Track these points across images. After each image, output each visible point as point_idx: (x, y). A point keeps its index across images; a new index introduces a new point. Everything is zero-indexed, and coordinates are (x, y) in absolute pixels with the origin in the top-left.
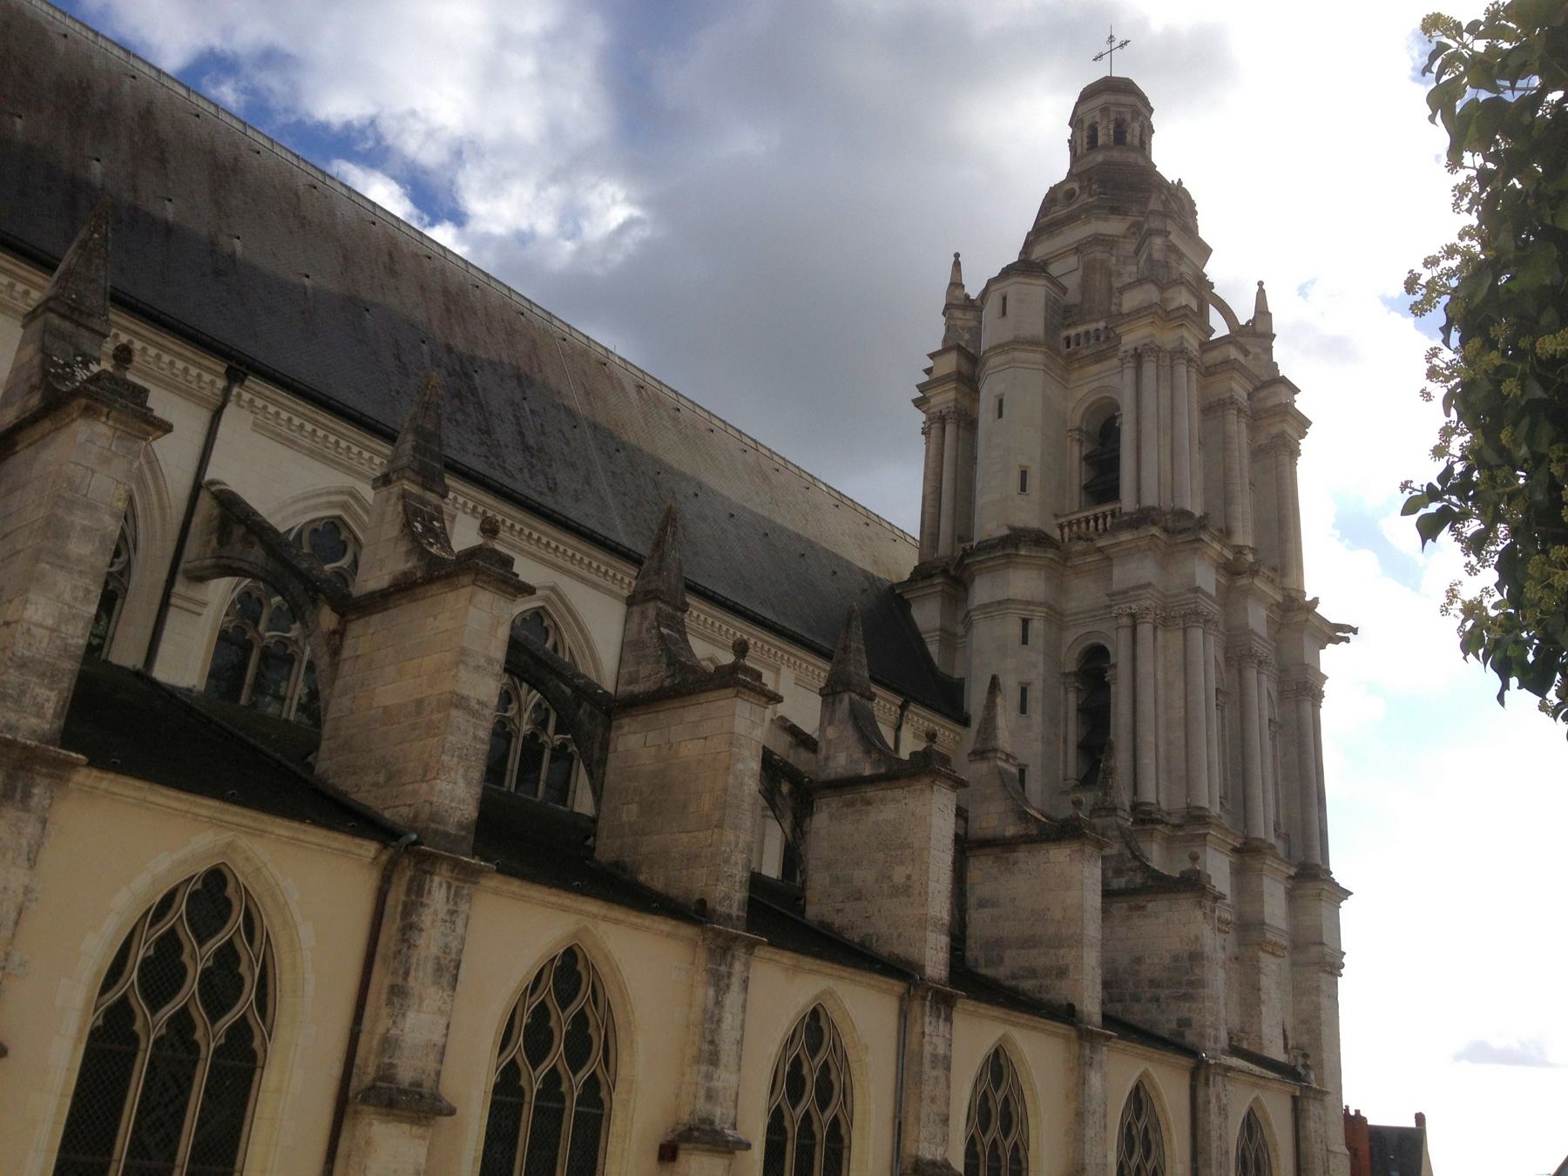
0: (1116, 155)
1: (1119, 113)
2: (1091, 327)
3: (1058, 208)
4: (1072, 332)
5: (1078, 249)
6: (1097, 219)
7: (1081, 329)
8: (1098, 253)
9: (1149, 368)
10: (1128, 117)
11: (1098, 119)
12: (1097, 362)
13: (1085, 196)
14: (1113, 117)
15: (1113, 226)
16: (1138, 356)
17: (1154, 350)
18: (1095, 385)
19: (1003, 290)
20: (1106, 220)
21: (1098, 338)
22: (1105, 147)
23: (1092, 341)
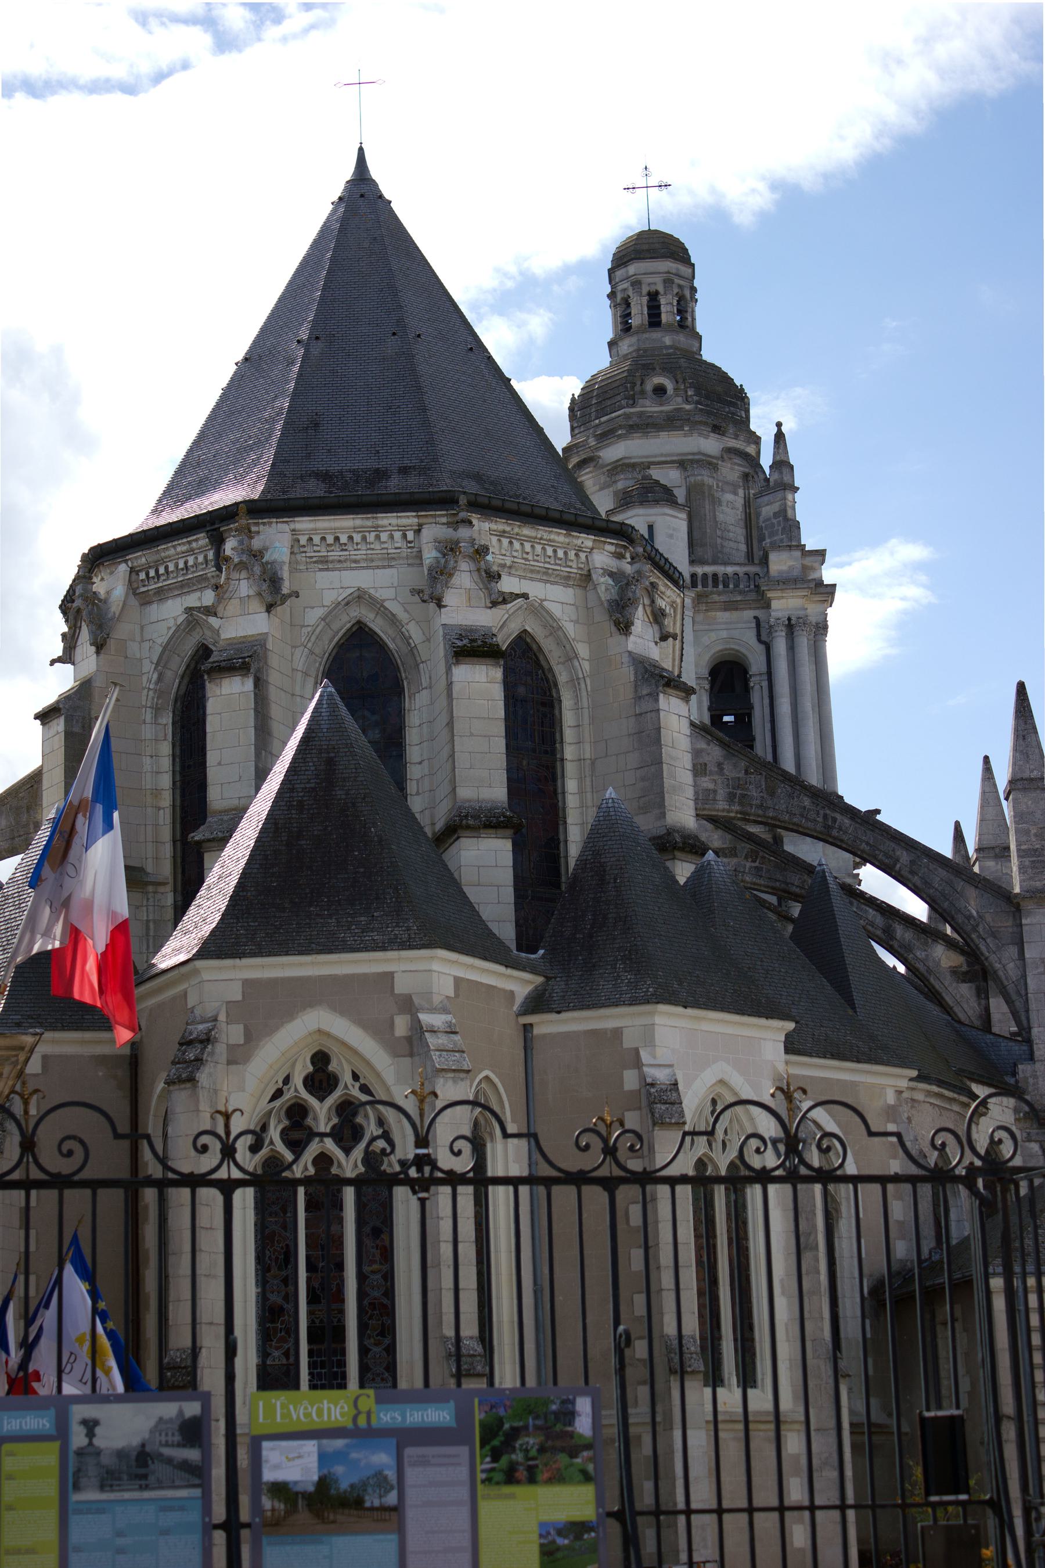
0: (682, 339)
1: (680, 286)
2: (720, 569)
3: (647, 402)
4: (700, 570)
5: (682, 464)
6: (700, 435)
7: (709, 569)
8: (704, 477)
9: (803, 642)
10: (687, 293)
11: (661, 289)
12: (725, 610)
13: (679, 400)
14: (676, 290)
15: (710, 445)
16: (790, 627)
17: (803, 621)
18: (724, 634)
19: (651, 519)
20: (707, 437)
21: (726, 585)
22: (670, 329)
23: (721, 587)
